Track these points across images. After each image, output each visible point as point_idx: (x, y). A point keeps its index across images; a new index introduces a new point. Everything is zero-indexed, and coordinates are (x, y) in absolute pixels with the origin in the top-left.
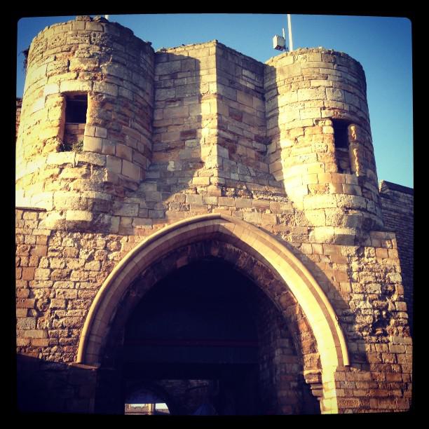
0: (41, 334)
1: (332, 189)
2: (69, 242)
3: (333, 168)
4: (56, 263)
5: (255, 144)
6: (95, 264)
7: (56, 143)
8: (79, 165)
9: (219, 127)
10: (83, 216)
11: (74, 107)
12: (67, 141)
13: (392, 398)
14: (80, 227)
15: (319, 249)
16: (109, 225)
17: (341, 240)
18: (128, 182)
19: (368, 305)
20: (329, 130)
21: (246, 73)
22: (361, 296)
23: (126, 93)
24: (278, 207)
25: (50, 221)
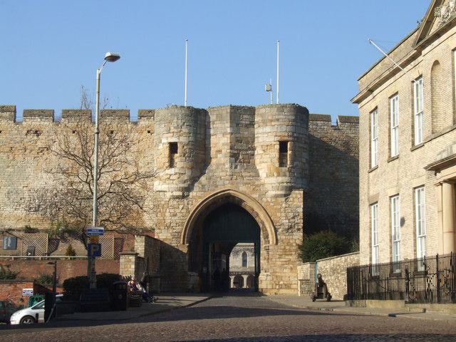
0: (169, 235)
1: (275, 175)
4: (172, 211)
6: (184, 211)
7: (167, 164)
8: (176, 174)
9: (231, 149)
10: (180, 193)
11: (173, 147)
12: (171, 164)
13: (291, 255)
14: (178, 197)
17: (277, 196)
19: (287, 221)
20: (277, 147)
21: (245, 116)
25: (169, 195)
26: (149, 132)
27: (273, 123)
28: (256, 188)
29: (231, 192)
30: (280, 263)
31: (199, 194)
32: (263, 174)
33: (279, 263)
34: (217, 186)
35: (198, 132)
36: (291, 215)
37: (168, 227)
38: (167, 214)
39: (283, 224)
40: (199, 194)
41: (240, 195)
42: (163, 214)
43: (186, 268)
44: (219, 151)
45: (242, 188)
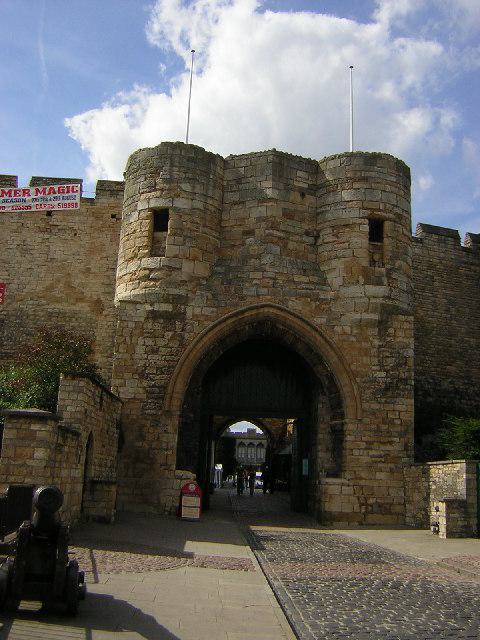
0: (141, 390)
2: (158, 327)
3: (365, 263)
4: (149, 342)
5: (305, 238)
6: (175, 344)
10: (168, 307)
11: (159, 218)
12: (155, 249)
13: (391, 443)
15: (348, 329)
16: (185, 313)
18: (198, 279)
20: (366, 228)
21: (300, 173)
22: (377, 368)
23: (199, 205)
24: (318, 294)
26: (113, 216)
27: (356, 185)
28: (322, 306)
29: (266, 310)
30: (368, 459)
31: (207, 311)
32: (335, 278)
33: (366, 459)
34: (242, 298)
35: (210, 194)
36: (391, 362)
37: (143, 376)
38: (140, 350)
39: (374, 380)
40: (207, 311)
41: (291, 318)
42: (131, 349)
43: (173, 461)
44: (250, 233)
45: (294, 305)
